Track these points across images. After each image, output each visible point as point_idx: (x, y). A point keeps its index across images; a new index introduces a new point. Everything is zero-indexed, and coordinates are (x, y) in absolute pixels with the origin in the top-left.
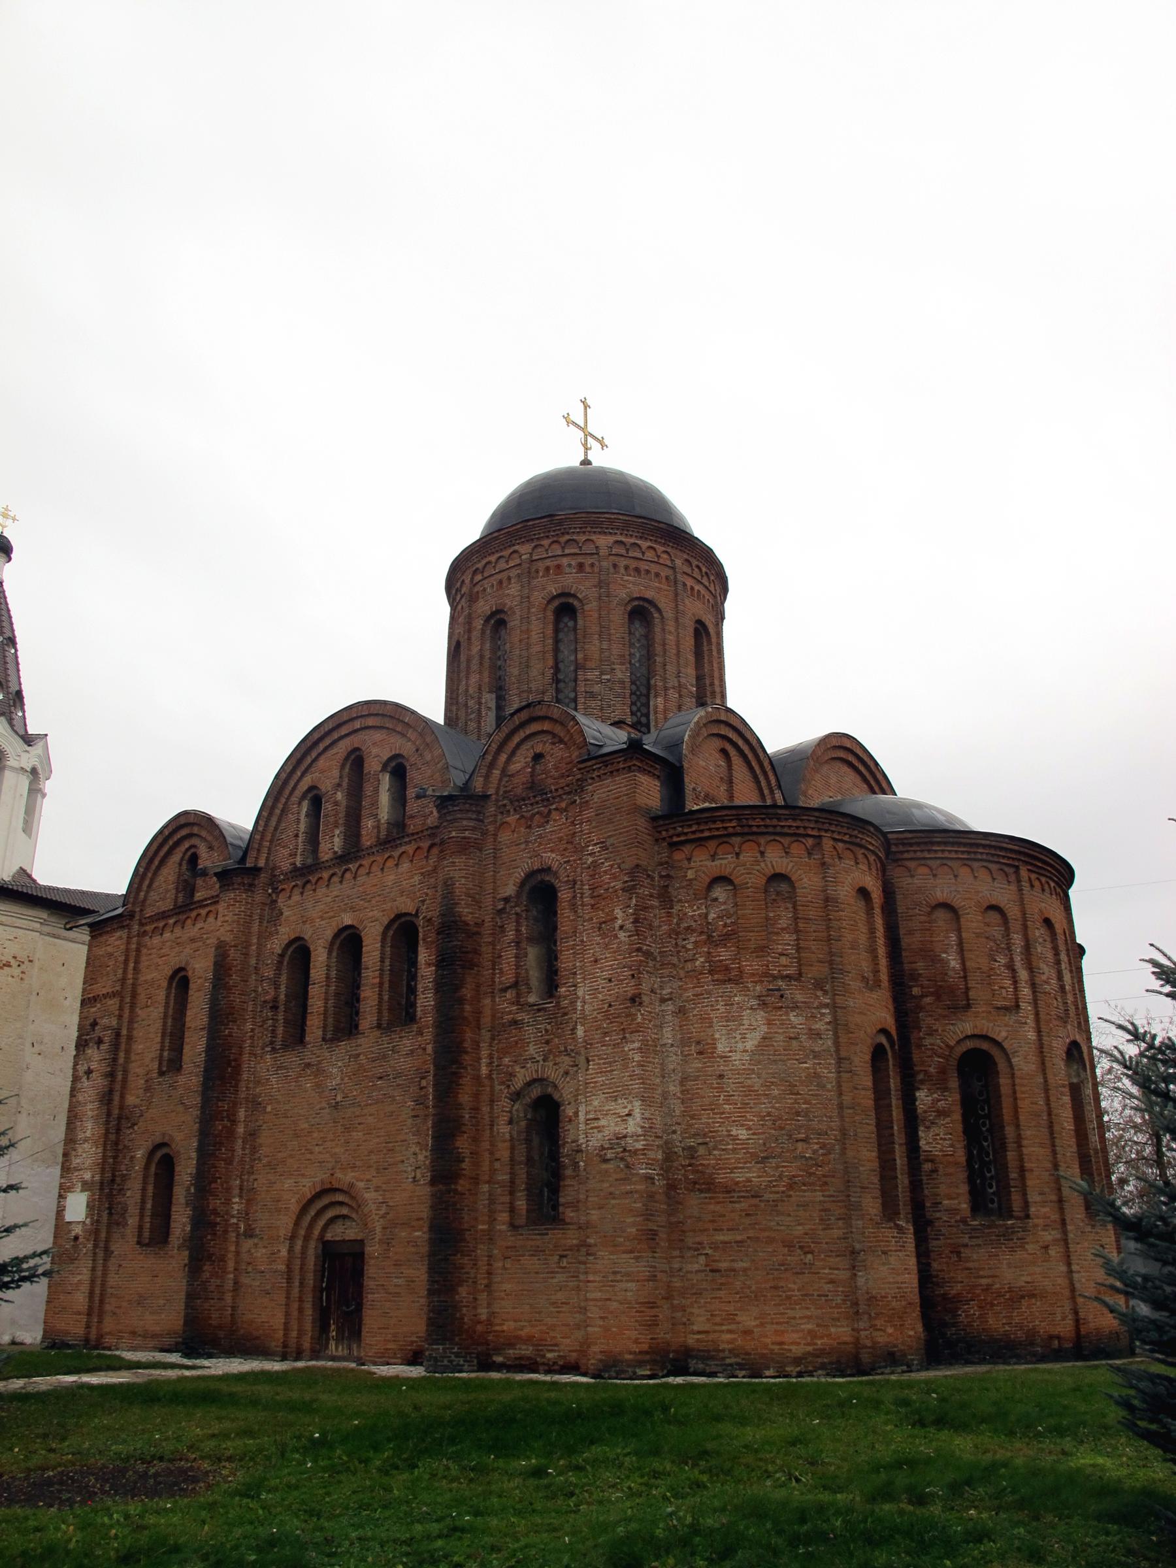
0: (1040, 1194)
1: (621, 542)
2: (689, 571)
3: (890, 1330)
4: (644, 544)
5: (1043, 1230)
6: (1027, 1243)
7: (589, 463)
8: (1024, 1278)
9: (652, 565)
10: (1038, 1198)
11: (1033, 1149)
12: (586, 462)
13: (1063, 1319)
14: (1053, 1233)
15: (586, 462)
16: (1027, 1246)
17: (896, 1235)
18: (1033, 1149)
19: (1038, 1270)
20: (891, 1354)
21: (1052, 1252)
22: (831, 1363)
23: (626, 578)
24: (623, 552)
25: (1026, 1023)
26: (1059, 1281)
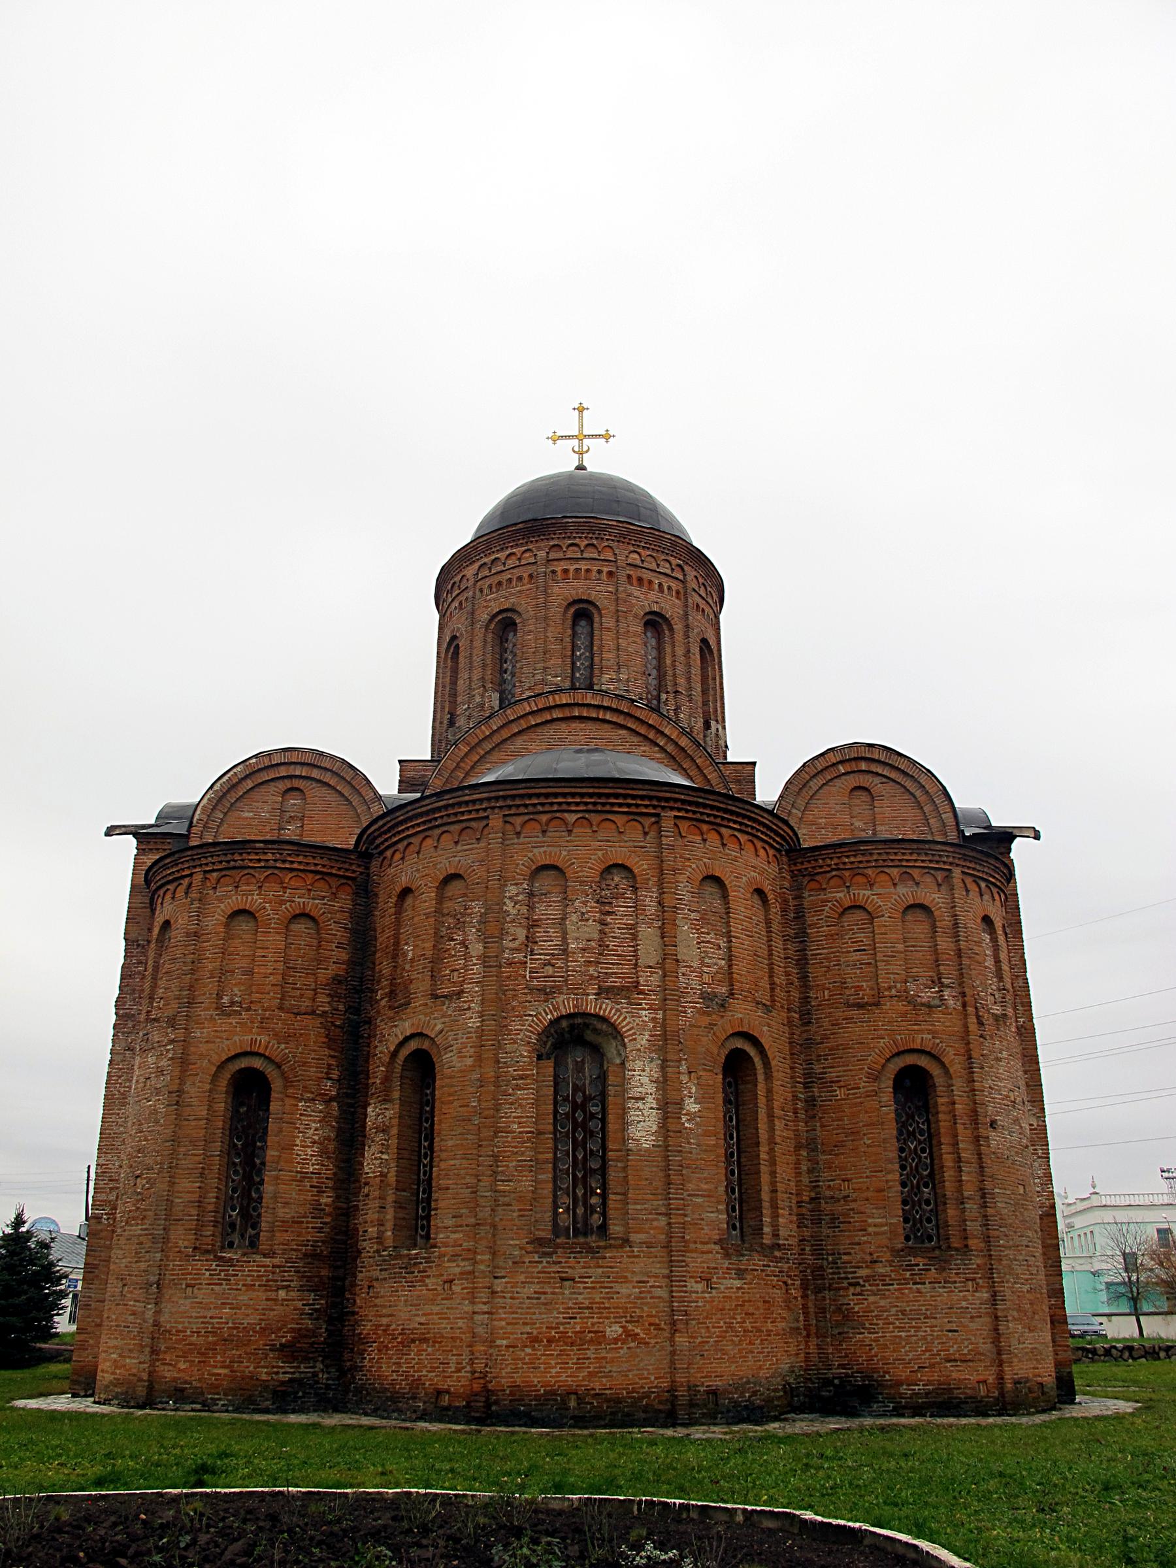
0: (454, 1217)
1: (485, 564)
2: (560, 555)
3: (182, 1366)
4: (502, 555)
5: (449, 1261)
6: (429, 1277)
7: (584, 468)
8: (418, 1319)
9: (514, 571)
10: (450, 1222)
11: (452, 1162)
12: (581, 467)
13: (458, 1370)
14: (462, 1264)
15: (581, 467)
16: (427, 1281)
17: (214, 1267)
18: (452, 1162)
19: (436, 1309)
20: (182, 1390)
21: (456, 1288)
22: (122, 1394)
23: (489, 597)
24: (486, 573)
25: (469, 1008)
26: (460, 1323)
